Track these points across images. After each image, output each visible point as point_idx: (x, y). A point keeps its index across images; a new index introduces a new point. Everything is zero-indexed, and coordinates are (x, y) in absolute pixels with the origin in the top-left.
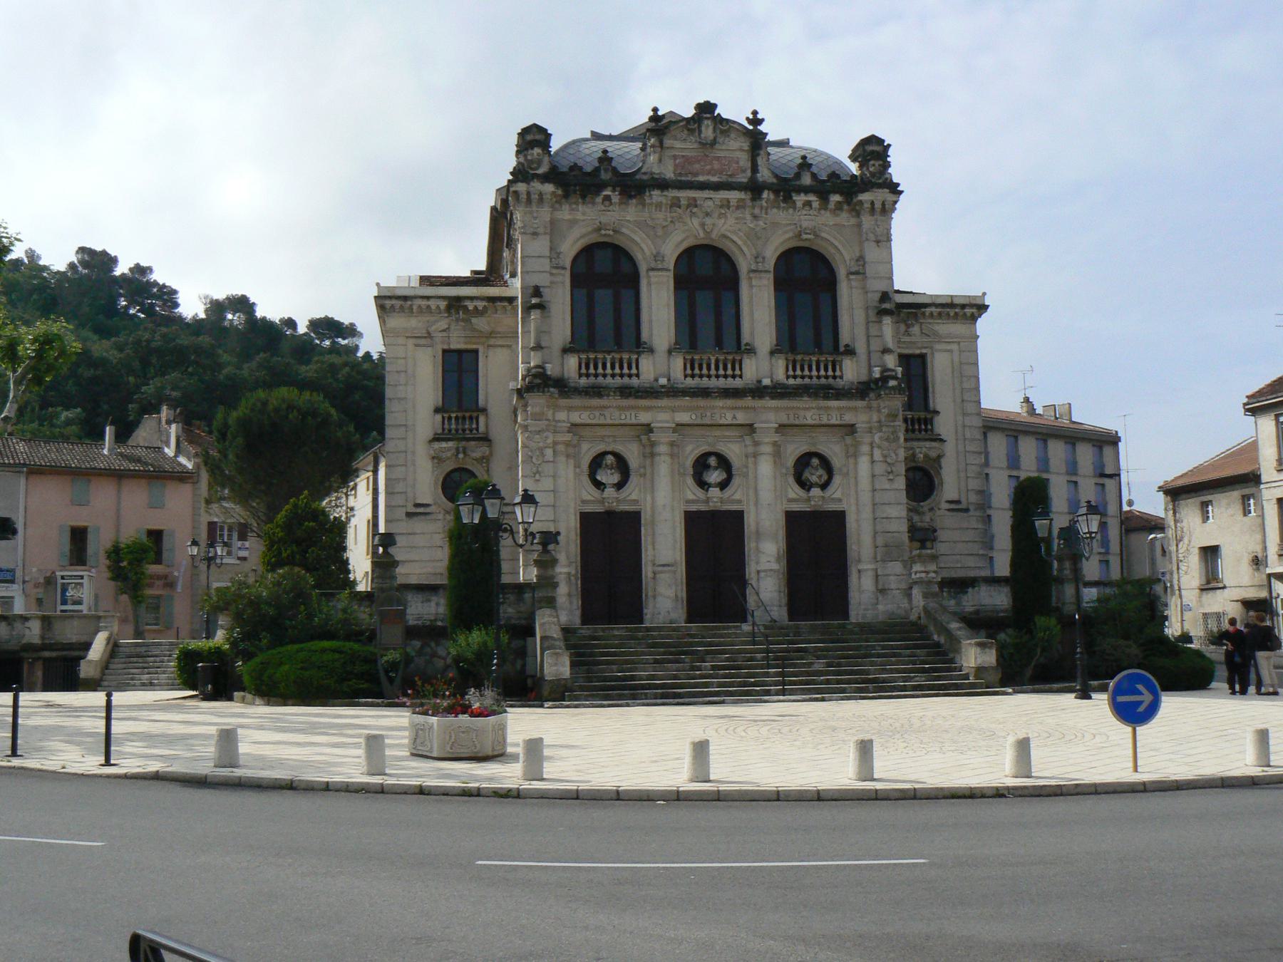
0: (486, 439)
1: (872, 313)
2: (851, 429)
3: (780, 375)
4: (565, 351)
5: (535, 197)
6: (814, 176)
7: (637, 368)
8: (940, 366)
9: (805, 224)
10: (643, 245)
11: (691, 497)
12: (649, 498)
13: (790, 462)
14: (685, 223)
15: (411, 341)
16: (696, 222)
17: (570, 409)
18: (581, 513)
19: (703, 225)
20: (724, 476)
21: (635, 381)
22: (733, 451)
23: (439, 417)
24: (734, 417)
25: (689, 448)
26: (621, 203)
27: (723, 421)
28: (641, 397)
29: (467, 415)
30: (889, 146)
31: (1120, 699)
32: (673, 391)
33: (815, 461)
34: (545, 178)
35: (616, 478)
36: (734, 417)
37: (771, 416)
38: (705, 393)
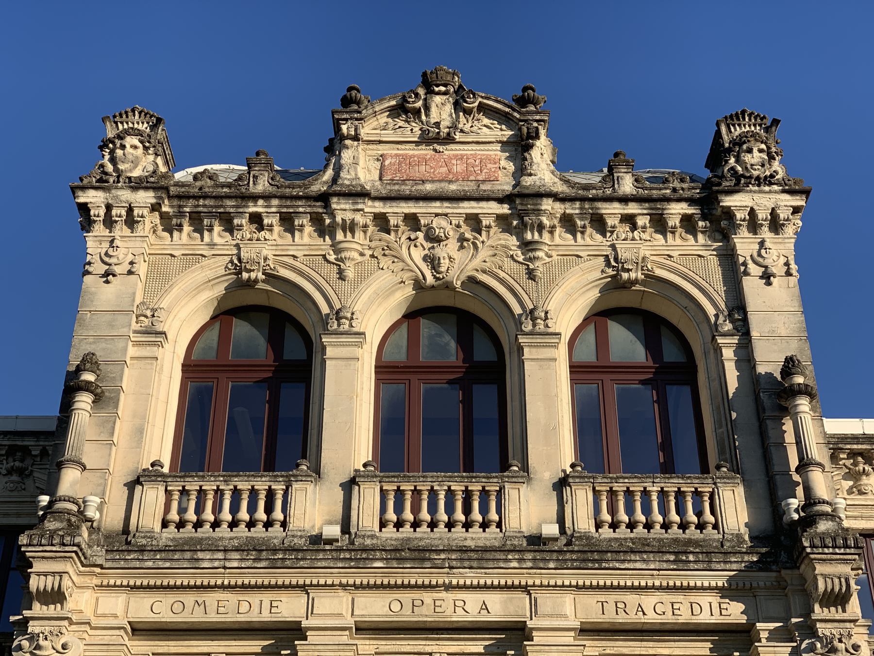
3: (582, 520)
5: (119, 212)
16: (418, 254)
24: (485, 607)
27: (459, 617)
34: (137, 185)
38: (420, 555)
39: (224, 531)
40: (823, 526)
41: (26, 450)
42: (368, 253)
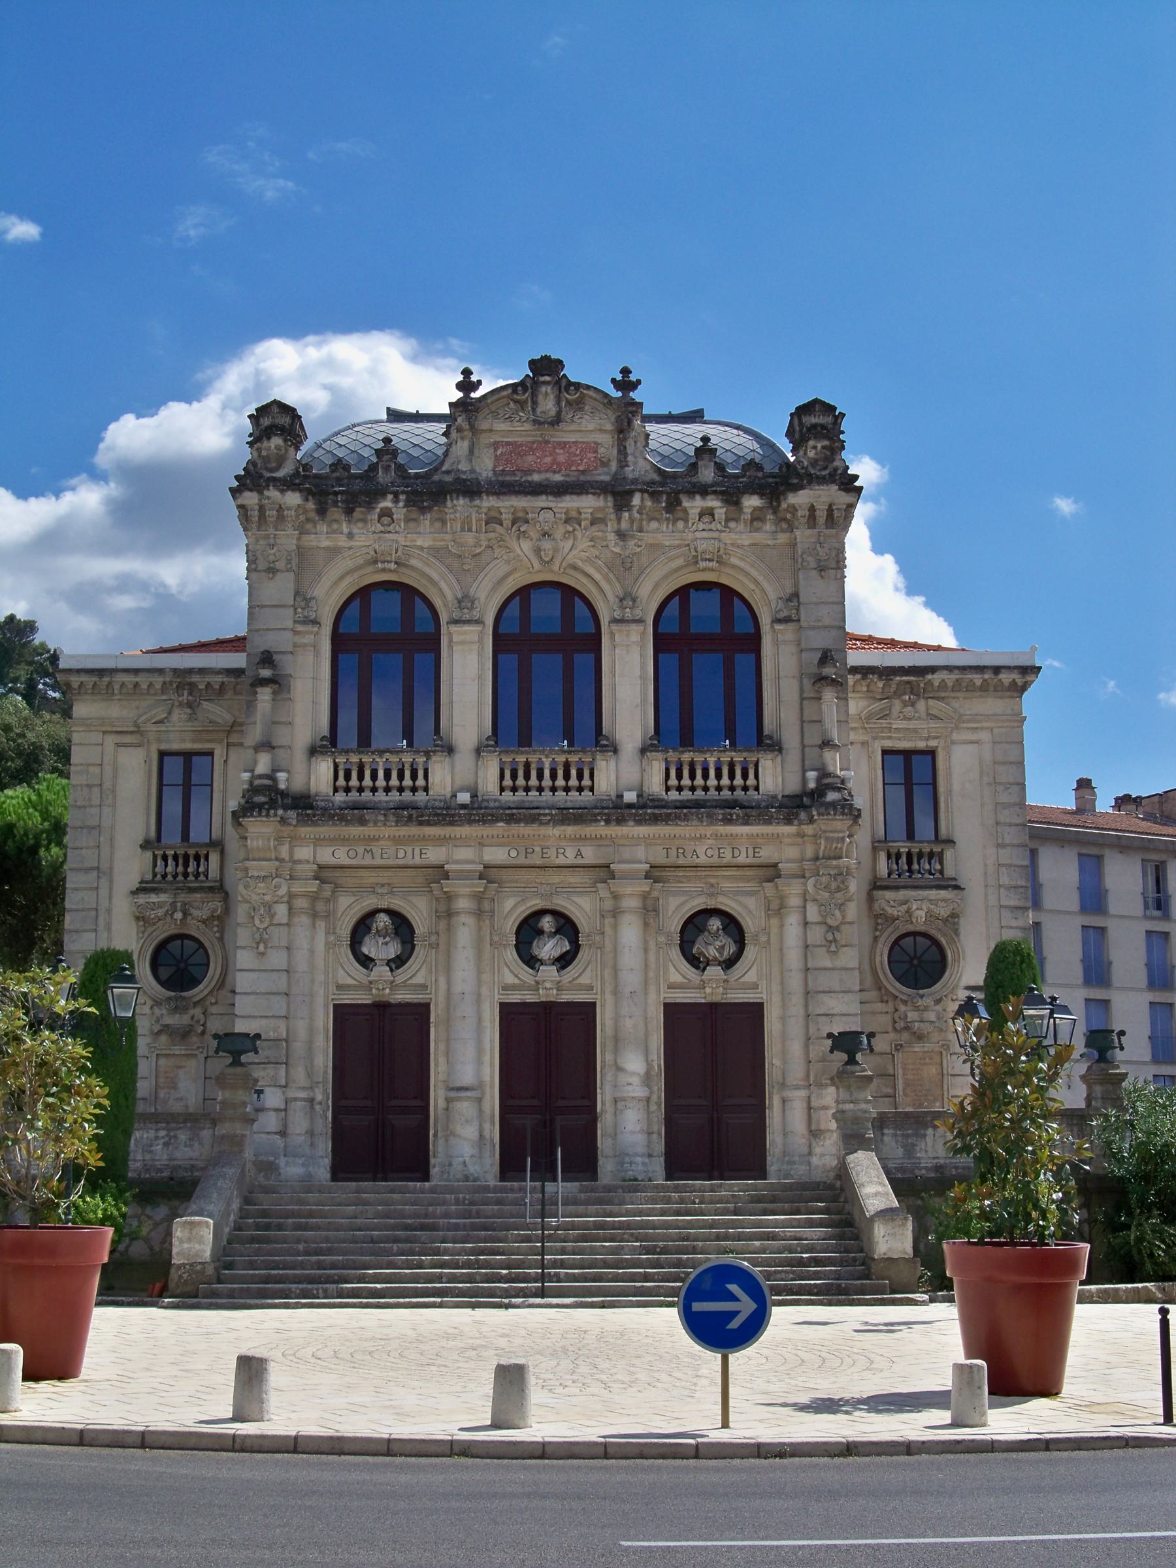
0: (220, 889)
1: (807, 683)
2: (771, 872)
3: (655, 785)
4: (314, 751)
5: (271, 514)
6: (720, 467)
7: (756, 776)
8: (961, 768)
9: (702, 546)
10: (443, 585)
11: (510, 979)
12: (442, 981)
13: (675, 924)
14: (510, 550)
15: (110, 740)
17: (318, 842)
18: (503, 1005)
19: (538, 551)
20: (566, 946)
21: (421, 796)
22: (581, 908)
23: (149, 855)
24: (579, 854)
25: (509, 903)
26: (408, 520)
27: (561, 860)
28: (428, 823)
29: (191, 852)
30: (843, 415)
31: (697, 1307)
32: (478, 811)
33: (715, 924)
35: (393, 949)
36: (579, 854)
37: (640, 852)
39: (381, 796)
40: (832, 796)
41: (192, 687)
42: (484, 543)
